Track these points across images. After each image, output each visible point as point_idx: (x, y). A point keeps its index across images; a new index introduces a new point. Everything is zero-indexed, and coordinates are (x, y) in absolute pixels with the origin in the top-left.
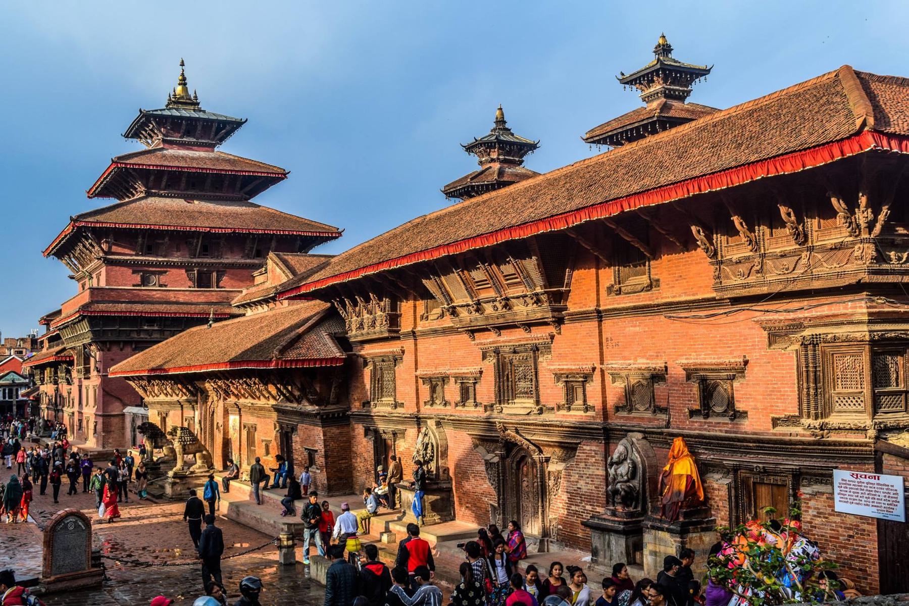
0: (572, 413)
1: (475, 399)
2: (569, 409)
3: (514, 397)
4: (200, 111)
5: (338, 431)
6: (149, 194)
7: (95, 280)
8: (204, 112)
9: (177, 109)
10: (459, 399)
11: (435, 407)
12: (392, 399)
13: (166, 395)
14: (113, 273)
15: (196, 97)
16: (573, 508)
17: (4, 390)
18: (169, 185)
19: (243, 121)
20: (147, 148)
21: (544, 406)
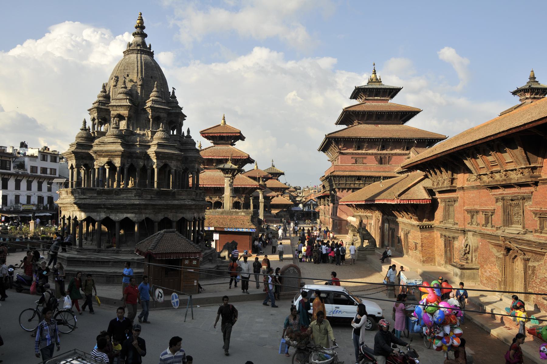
0: (542, 235)
1: (491, 223)
2: (541, 233)
3: (512, 224)
4: (382, 85)
5: (428, 234)
6: (359, 123)
7: (337, 161)
8: (384, 85)
9: (371, 85)
10: (484, 223)
11: (473, 226)
12: (453, 220)
13: (362, 212)
14: (343, 158)
15: (380, 79)
16: (542, 288)
17: (309, 207)
18: (368, 119)
19: (401, 88)
20: (359, 103)
21: (527, 230)
